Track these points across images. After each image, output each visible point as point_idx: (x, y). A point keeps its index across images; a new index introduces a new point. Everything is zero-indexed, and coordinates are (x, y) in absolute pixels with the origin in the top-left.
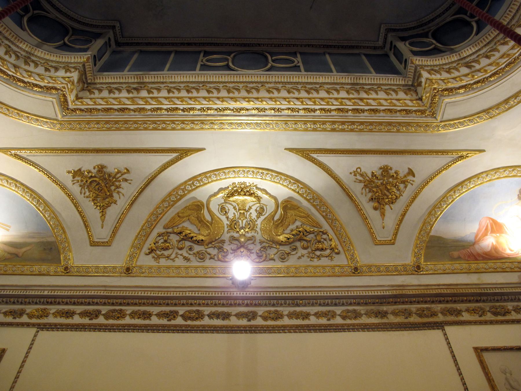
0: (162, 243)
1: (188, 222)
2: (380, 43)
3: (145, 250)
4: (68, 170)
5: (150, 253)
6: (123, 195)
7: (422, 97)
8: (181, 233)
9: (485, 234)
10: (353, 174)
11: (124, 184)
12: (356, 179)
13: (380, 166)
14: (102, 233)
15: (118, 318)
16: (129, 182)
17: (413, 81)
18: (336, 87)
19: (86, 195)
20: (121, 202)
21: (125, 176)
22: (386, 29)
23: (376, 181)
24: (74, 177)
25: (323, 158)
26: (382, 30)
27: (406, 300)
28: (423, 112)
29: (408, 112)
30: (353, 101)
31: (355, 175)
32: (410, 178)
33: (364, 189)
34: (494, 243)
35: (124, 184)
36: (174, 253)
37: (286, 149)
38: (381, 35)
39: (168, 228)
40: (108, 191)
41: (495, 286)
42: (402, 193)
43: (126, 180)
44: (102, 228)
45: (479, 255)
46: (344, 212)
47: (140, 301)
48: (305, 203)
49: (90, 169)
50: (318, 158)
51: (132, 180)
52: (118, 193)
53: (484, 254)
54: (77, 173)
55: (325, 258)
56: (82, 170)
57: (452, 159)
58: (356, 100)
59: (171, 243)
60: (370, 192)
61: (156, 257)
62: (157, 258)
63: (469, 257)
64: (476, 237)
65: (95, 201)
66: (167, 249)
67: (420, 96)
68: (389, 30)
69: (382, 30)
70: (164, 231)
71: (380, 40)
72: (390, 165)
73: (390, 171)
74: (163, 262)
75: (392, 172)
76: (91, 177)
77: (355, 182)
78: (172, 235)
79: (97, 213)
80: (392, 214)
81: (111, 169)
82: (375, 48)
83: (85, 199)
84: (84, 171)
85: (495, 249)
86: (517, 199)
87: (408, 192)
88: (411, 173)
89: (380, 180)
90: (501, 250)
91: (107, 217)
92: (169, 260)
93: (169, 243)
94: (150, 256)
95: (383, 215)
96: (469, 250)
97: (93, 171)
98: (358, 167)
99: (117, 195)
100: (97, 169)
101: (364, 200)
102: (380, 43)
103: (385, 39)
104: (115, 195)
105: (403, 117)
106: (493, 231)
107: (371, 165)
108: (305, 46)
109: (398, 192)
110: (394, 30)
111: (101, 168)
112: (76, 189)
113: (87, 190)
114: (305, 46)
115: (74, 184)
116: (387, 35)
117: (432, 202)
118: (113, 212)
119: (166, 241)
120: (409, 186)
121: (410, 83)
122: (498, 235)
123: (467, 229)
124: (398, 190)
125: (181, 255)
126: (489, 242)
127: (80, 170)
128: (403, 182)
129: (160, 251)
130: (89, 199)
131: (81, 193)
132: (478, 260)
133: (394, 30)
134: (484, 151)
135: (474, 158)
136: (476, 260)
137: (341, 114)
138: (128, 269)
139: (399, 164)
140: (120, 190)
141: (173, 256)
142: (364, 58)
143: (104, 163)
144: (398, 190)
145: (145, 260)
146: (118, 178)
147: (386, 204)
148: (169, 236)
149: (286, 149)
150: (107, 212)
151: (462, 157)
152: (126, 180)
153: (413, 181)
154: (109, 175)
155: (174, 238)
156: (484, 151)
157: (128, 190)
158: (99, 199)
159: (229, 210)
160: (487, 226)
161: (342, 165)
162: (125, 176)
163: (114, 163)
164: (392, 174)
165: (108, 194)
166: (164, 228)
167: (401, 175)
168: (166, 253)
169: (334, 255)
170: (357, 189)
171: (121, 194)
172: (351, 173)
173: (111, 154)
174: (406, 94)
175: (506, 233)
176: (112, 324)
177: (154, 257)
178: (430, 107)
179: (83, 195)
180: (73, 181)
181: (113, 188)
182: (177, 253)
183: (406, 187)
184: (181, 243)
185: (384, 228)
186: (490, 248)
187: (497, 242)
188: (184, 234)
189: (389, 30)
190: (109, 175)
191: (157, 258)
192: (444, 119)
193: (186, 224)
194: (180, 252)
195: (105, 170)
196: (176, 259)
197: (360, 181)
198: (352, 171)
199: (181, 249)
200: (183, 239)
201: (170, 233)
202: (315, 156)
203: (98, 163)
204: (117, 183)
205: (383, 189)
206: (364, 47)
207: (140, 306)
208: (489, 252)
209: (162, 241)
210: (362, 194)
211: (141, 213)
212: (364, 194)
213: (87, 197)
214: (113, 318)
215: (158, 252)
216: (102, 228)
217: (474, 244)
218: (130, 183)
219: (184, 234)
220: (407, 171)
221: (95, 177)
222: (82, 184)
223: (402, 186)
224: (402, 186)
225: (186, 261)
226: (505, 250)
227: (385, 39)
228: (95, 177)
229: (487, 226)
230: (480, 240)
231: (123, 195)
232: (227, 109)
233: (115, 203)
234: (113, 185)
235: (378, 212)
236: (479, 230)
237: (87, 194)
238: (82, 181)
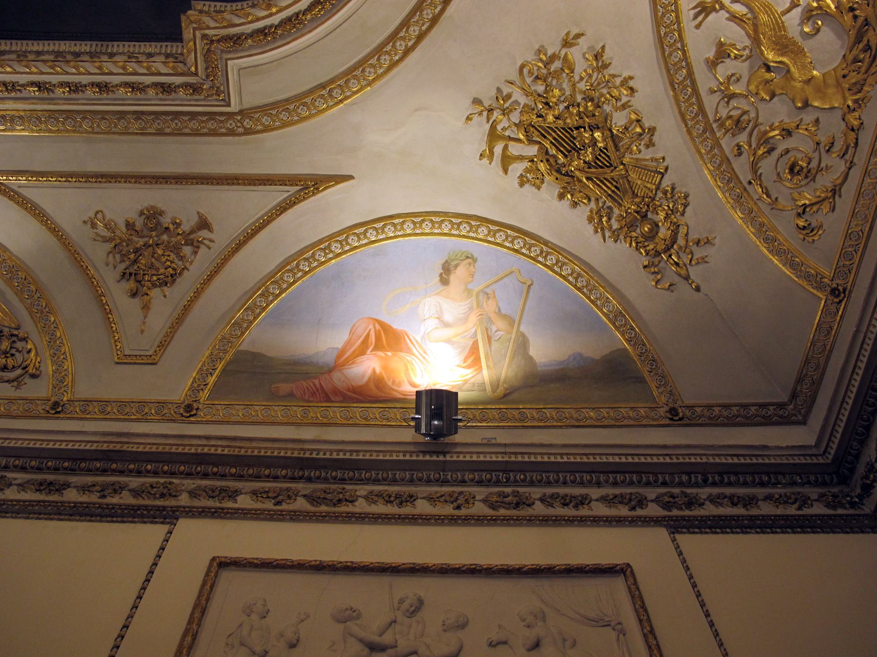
9: (362, 351)
10: (89, 223)
23: (135, 239)
27: (132, 466)
28: (195, 89)
29: (166, 89)
31: (94, 226)
32: (204, 233)
33: (111, 256)
34: (378, 371)
41: (340, 447)
42: (188, 265)
45: (336, 392)
46: (69, 299)
53: (349, 390)
55: (6, 384)
57: (286, 195)
60: (122, 261)
63: (313, 394)
64: (339, 357)
72: (160, 206)
73: (162, 219)
75: (166, 221)
77: (95, 240)
80: (163, 304)
85: (378, 381)
86: (439, 283)
87: (200, 263)
88: (204, 224)
89: (142, 237)
90: (390, 383)
95: (146, 307)
96: (317, 382)
98: (98, 209)
101: (110, 278)
105: (161, 100)
106: (378, 347)
107: (124, 204)
109: (180, 263)
117: (252, 285)
120: (203, 250)
122: (389, 354)
123: (326, 341)
124: (182, 258)
126: (368, 366)
128: (190, 243)
132: (332, 402)
135: (331, 194)
136: (328, 400)
139: (180, 205)
144: (182, 258)
147: (154, 286)
153: (212, 241)
156: (351, 177)
160: (368, 335)
161: (69, 206)
164: (166, 225)
167: (186, 227)
169: (27, 379)
170: (98, 254)
172: (85, 222)
175: (409, 351)
178: (208, 76)
183: (196, 253)
185: (142, 332)
186: (366, 379)
187: (385, 368)
197: (106, 240)
198: (86, 218)
205: (151, 254)
208: (361, 386)
210: (107, 265)
212: (111, 266)
217: (330, 370)
220: (195, 219)
223: (187, 250)
224: (187, 250)
226: (399, 385)
229: (368, 335)
230: (346, 362)
235: (136, 301)
236: (348, 343)
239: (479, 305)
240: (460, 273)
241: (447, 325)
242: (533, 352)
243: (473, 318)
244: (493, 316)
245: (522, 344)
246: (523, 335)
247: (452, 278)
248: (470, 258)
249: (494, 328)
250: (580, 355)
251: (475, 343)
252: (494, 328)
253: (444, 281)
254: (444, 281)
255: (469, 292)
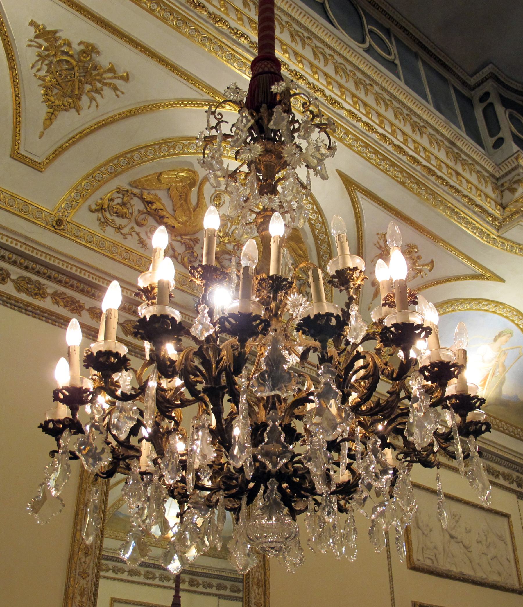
0: (118, 204)
1: (166, 193)
2: (472, 81)
3: (93, 201)
4: (35, 20)
5: (96, 211)
6: (97, 106)
7: (507, 206)
8: (151, 203)
11: (107, 91)
12: (378, 243)
13: (409, 242)
14: (37, 147)
15: (36, 294)
16: (118, 93)
17: (504, 176)
18: (436, 138)
19: (39, 73)
20: (88, 114)
21: (119, 83)
22: (491, 73)
24: (37, 37)
25: (364, 203)
26: (486, 71)
30: (450, 170)
35: (107, 91)
36: (130, 226)
37: (337, 170)
38: (481, 73)
39: (136, 187)
40: (79, 88)
43: (115, 88)
44: (40, 138)
47: (68, 280)
48: (310, 241)
49: (71, 40)
50: (361, 200)
51: (123, 93)
52: (92, 99)
54: (46, 35)
56: (58, 35)
58: (452, 171)
59: (130, 211)
61: (103, 220)
62: (104, 223)
65: (49, 92)
66: (122, 216)
67: (504, 202)
68: (494, 77)
69: (486, 71)
70: (128, 188)
71: (475, 77)
74: (110, 233)
76: (67, 54)
78: (135, 199)
79: (44, 110)
81: (103, 61)
82: (464, 83)
83: (35, 79)
84: (60, 38)
91: (56, 124)
92: (119, 234)
93: (128, 209)
94: (95, 215)
97: (75, 46)
99: (88, 100)
100: (82, 47)
102: (472, 80)
103: (482, 82)
104: (85, 99)
108: (401, 27)
110: (497, 80)
111: (89, 50)
112: (27, 56)
113: (45, 68)
114: (401, 27)
115: (29, 46)
116: (487, 79)
118: (69, 122)
119: (124, 204)
121: (497, 175)
125: (138, 234)
127: (56, 32)
129: (111, 215)
130: (41, 82)
131: (33, 66)
133: (497, 80)
134: (503, 280)
137: (425, 174)
138: (59, 222)
140: (97, 96)
141: (126, 230)
142: (452, 92)
143: (101, 47)
145: (85, 219)
146: (105, 79)
148: (132, 199)
149: (337, 170)
150: (59, 117)
151: (481, 277)
152: (115, 88)
154: (96, 67)
155: (137, 205)
157: (108, 103)
158: (56, 91)
159: (224, 202)
162: (119, 83)
163: (112, 53)
165: (76, 92)
166: (130, 184)
168: (119, 221)
171: (94, 103)
172: (378, 234)
173: (122, 42)
174: (494, 192)
176: (28, 303)
177: (99, 219)
179: (34, 70)
180: (31, 41)
181: (88, 87)
182: (132, 228)
184: (143, 216)
188: (154, 207)
189: (494, 77)
190: (95, 68)
191: (104, 223)
192: (503, 236)
193: (162, 194)
194: (137, 229)
195: (94, 55)
196: (129, 237)
199: (139, 225)
200: (149, 213)
201: (135, 195)
202: (359, 195)
203: (91, 41)
204: (99, 85)
206: (455, 75)
207: (66, 287)
209: (119, 201)
211: (108, 145)
213: (40, 78)
214: (28, 292)
215: (108, 215)
216: (40, 138)
218: (118, 96)
219: (154, 207)
221: (71, 56)
222: (43, 54)
225: (141, 245)
227: (482, 82)
228: (71, 56)
231: (97, 106)
232: (322, 91)
233: (78, 111)
234: (91, 84)
237: (43, 73)
238: (46, 49)
239: (499, 357)
240: (503, 339)
241: (483, 361)
242: (504, 388)
243: (493, 362)
244: (501, 364)
245: (502, 383)
246: (504, 378)
247: (499, 340)
248: (511, 334)
249: (497, 370)
250: (517, 396)
251: (488, 374)
252: (497, 370)
253: (495, 340)
254: (495, 340)
255: (500, 348)
